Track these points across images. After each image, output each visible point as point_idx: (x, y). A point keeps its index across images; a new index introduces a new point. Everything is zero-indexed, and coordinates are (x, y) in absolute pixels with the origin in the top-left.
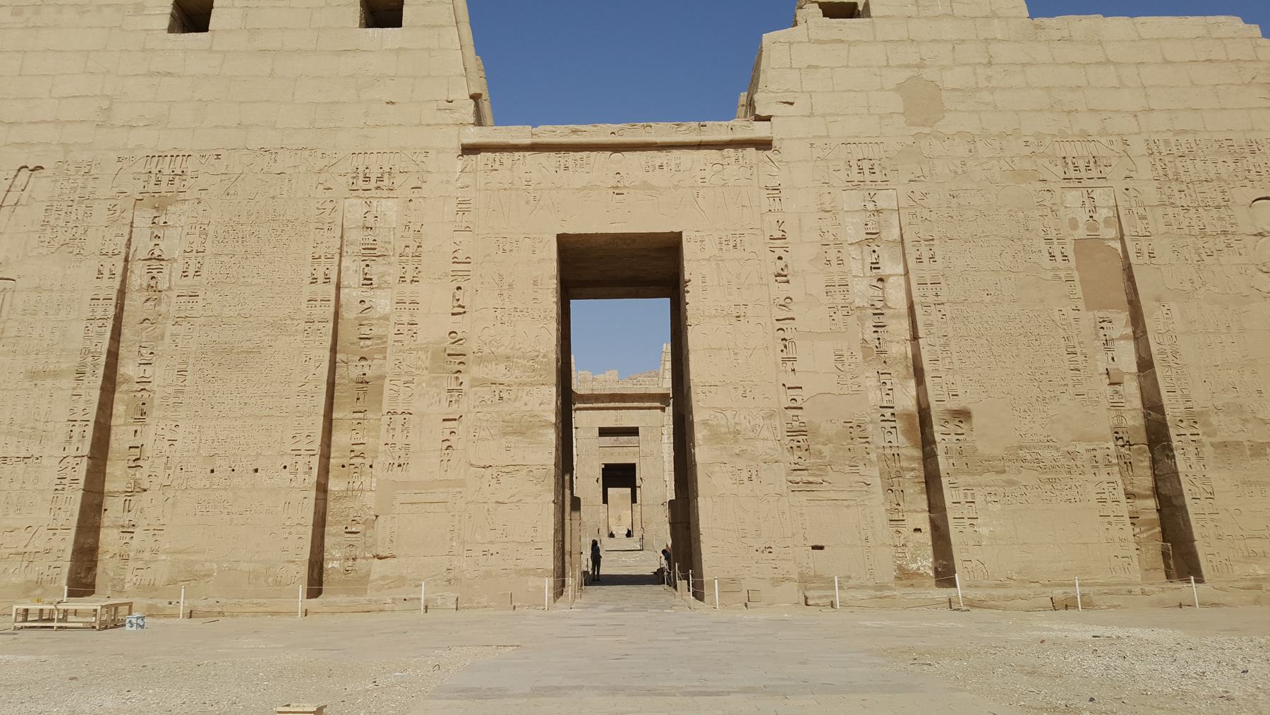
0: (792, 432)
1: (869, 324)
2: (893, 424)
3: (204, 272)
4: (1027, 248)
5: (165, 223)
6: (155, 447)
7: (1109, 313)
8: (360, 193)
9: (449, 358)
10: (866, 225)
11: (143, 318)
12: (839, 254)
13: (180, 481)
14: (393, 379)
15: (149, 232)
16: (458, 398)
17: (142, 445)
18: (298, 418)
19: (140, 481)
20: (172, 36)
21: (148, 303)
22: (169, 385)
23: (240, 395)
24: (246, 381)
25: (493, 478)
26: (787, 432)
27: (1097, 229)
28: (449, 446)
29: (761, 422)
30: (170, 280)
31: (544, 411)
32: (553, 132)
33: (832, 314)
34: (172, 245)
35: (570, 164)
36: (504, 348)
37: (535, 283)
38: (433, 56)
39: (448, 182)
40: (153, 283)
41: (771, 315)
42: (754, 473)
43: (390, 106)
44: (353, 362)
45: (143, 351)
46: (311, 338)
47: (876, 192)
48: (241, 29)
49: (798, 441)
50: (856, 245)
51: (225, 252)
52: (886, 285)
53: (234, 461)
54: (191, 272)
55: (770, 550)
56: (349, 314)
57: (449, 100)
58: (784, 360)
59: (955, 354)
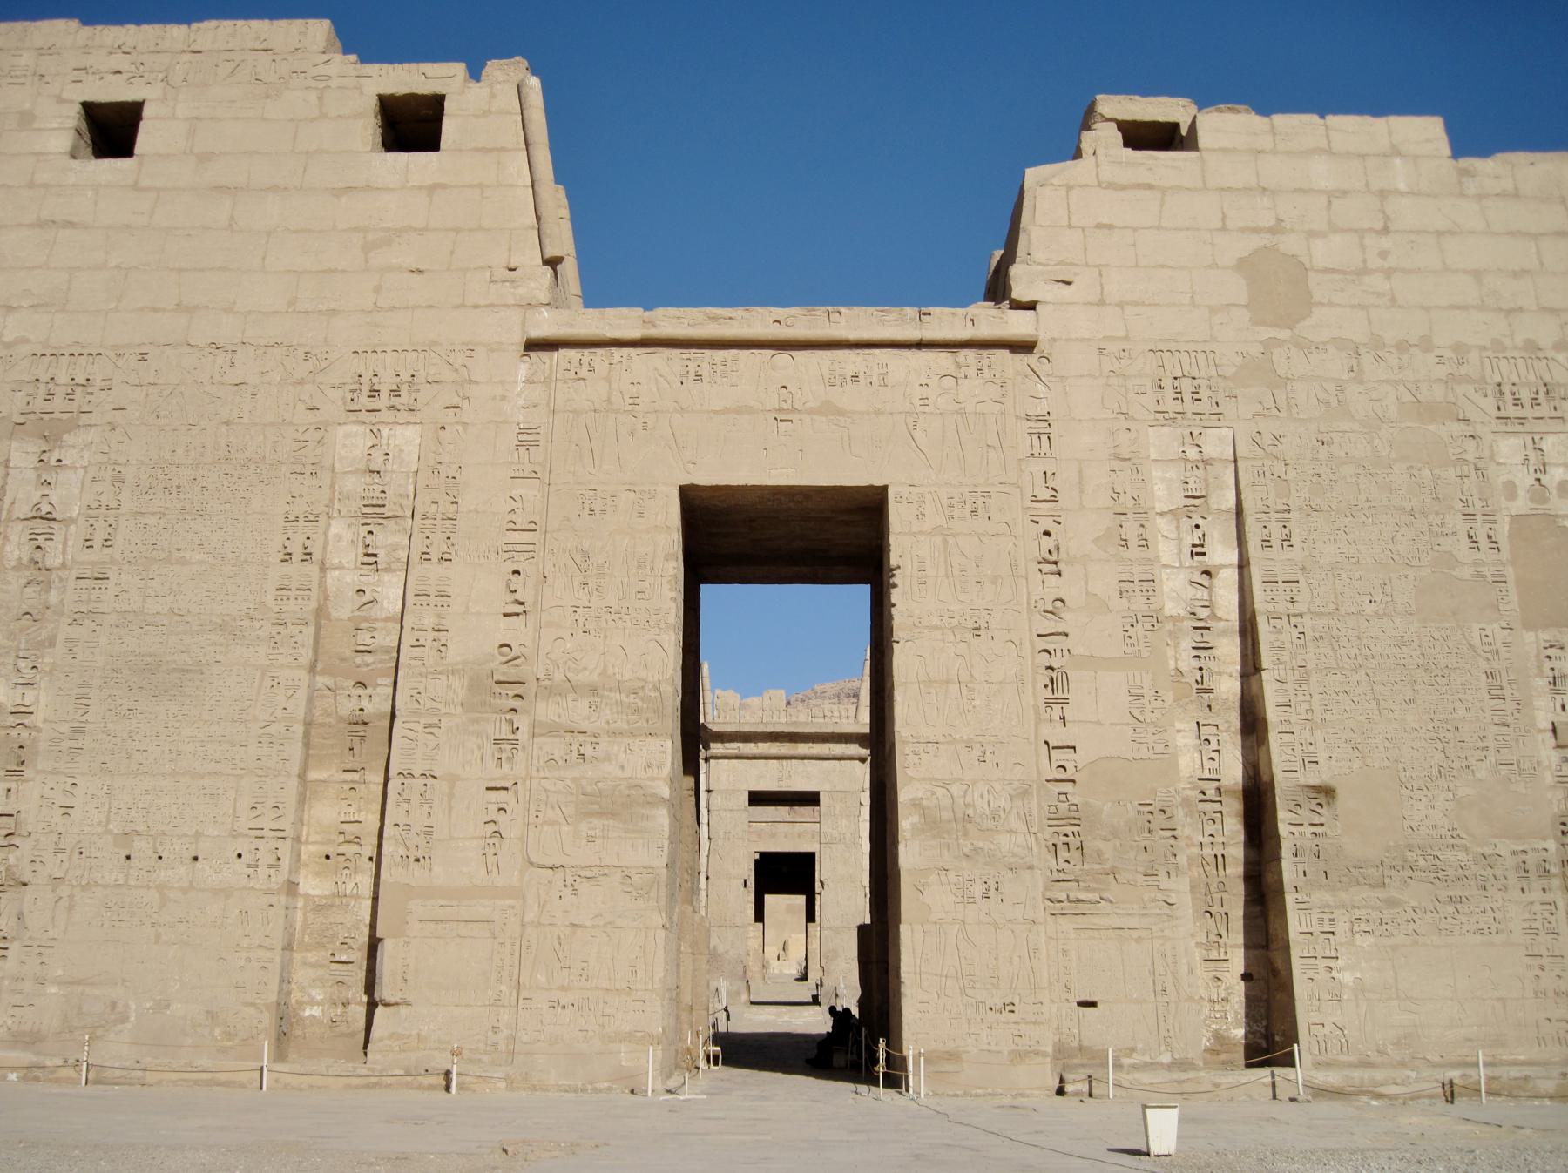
0: (1055, 820)
1: (1187, 643)
2: (1217, 807)
3: (119, 541)
4: (1435, 528)
5: (60, 460)
7: (1560, 633)
8: (364, 416)
9: (497, 688)
10: (1186, 483)
11: (22, 611)
12: (1142, 530)
13: (79, 872)
14: (408, 719)
15: (32, 475)
16: (510, 755)
18: (260, 779)
19: (15, 869)
20: (75, 164)
21: (29, 590)
22: (64, 720)
23: (172, 739)
24: (180, 717)
25: (565, 886)
27: (1546, 500)
28: (495, 832)
30: (64, 553)
31: (653, 779)
32: (678, 318)
33: (1128, 627)
34: (69, 495)
35: (705, 371)
36: (587, 673)
37: (641, 565)
38: (487, 198)
39: (503, 398)
40: (38, 555)
41: (1030, 627)
42: (993, 886)
43: (415, 275)
44: (344, 689)
45: (22, 664)
46: (282, 650)
47: (1202, 430)
48: (185, 153)
49: (1066, 835)
50: (1169, 517)
51: (151, 510)
52: (1215, 581)
53: (161, 844)
54: (98, 542)
55: (1011, 1008)
56: (343, 610)
57: (512, 266)
58: (1049, 702)
59: (1316, 696)
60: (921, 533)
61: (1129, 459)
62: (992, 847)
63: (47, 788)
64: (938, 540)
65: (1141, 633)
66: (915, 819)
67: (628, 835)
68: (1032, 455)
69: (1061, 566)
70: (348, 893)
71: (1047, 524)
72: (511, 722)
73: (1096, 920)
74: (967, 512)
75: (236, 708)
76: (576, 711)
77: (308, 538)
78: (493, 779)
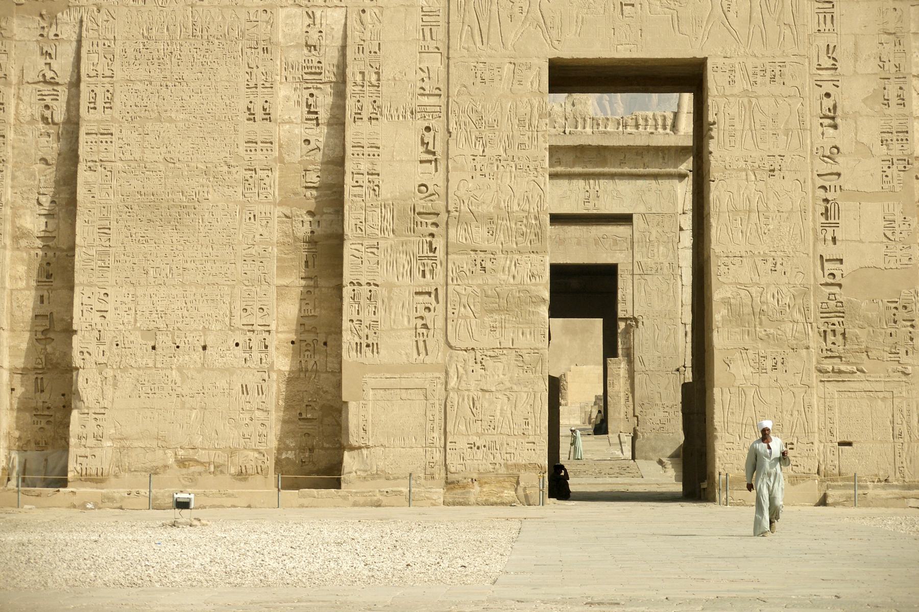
0: (825, 313)
6: (83, 319)
9: (418, 218)
12: (900, 92)
14: (354, 242)
17: (51, 313)
24: (182, 242)
25: (476, 363)
26: (821, 313)
28: (423, 325)
29: (788, 301)
31: (536, 285)
33: (885, 169)
36: (485, 206)
42: (779, 361)
49: (834, 324)
54: (100, 104)
60: (732, 95)
61: (894, 33)
62: (780, 332)
63: (85, 297)
64: (746, 100)
65: (896, 173)
66: (724, 312)
67: (520, 326)
68: (819, 30)
69: (838, 121)
70: (310, 368)
71: (828, 87)
72: (431, 244)
73: (852, 385)
74: (768, 78)
75: (224, 235)
76: (479, 235)
77: (266, 102)
78: (419, 286)
